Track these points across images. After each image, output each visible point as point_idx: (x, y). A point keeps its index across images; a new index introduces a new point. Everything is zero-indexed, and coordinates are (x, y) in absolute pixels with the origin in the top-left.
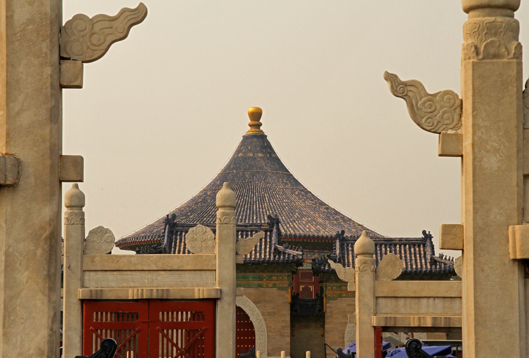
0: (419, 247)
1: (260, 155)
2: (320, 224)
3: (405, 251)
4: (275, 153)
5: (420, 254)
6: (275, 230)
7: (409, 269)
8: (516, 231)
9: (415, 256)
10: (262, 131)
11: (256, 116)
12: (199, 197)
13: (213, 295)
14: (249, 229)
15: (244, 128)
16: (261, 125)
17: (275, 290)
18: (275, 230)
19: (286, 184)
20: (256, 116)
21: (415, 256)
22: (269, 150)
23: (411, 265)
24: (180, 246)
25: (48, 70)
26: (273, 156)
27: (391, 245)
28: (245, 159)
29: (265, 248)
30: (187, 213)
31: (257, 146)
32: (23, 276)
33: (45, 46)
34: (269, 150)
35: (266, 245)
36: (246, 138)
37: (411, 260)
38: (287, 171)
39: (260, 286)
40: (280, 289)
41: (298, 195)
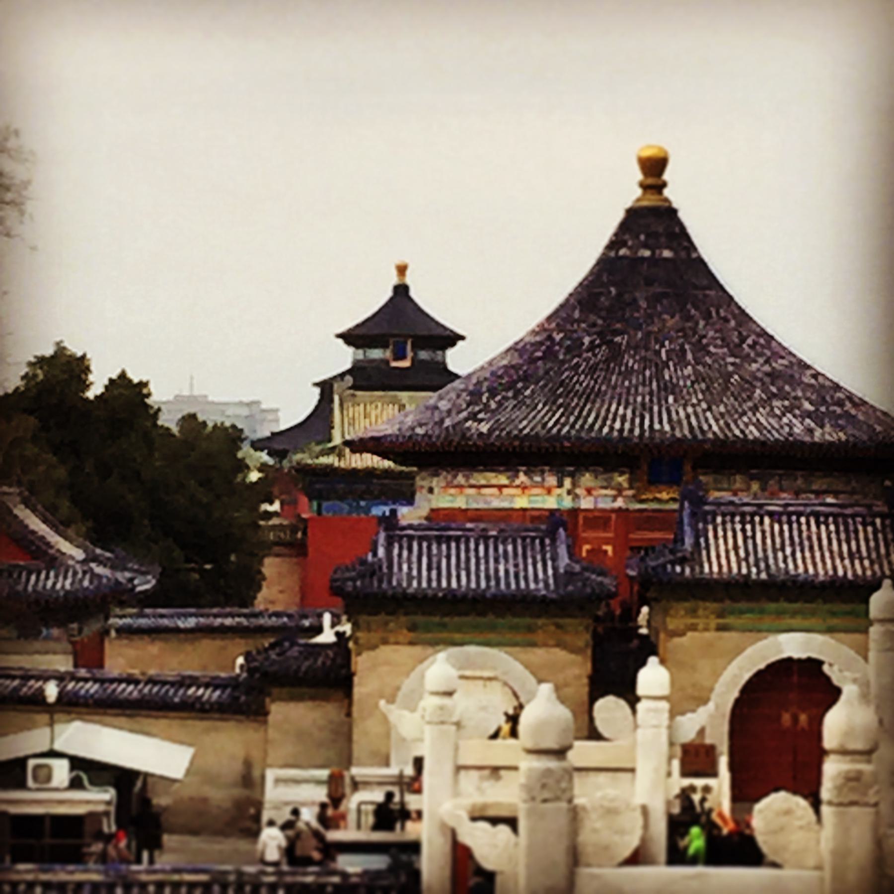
1: (667, 254)
2: (809, 415)
4: (695, 249)
10: (666, 200)
11: (654, 168)
14: (849, 511)
15: (628, 191)
16: (664, 185)
19: (726, 320)
20: (654, 168)
22: (686, 244)
24: (717, 547)
36: (632, 214)
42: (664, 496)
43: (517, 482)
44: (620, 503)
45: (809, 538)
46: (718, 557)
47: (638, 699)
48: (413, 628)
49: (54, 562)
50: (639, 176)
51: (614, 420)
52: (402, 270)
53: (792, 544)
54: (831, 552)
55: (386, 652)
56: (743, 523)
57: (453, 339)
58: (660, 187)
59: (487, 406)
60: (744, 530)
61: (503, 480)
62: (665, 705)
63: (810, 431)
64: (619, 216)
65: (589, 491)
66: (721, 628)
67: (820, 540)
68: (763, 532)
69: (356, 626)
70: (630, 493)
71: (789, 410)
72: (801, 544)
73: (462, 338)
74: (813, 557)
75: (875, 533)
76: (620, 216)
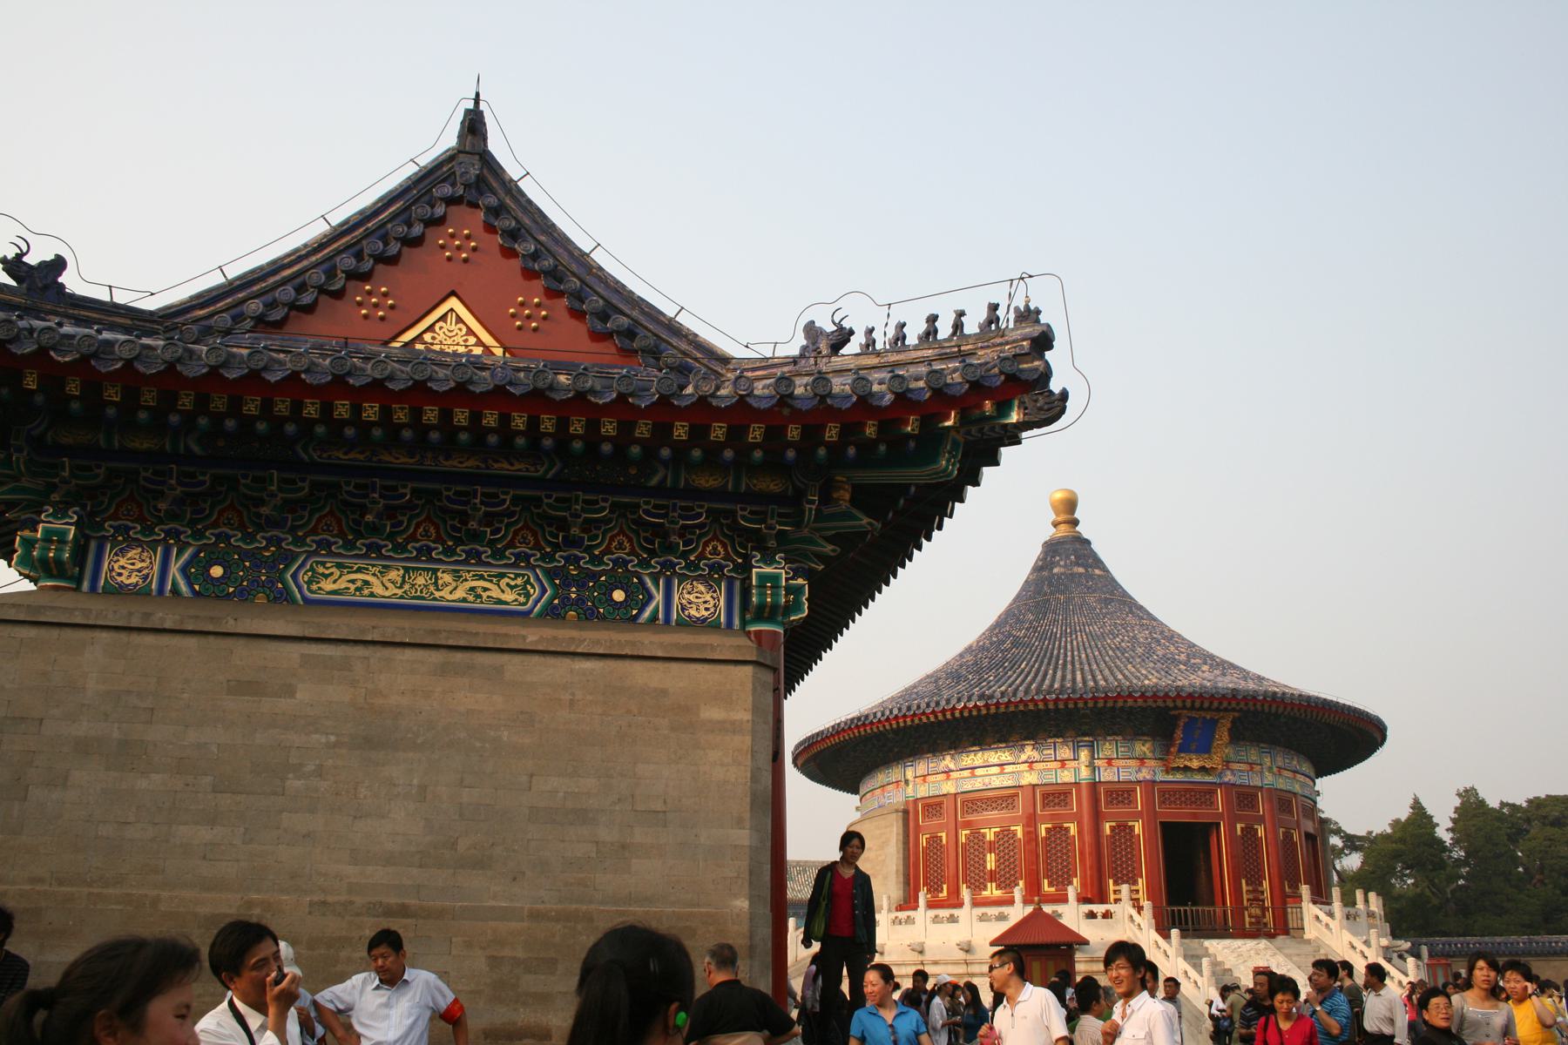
15: (1044, 529)
20: (1070, 505)
36: (1052, 549)
42: (1195, 764)
43: (1024, 757)
44: (1145, 774)
58: (1075, 523)
61: (1005, 756)
65: (1110, 761)
70: (1153, 763)
76: (1037, 551)
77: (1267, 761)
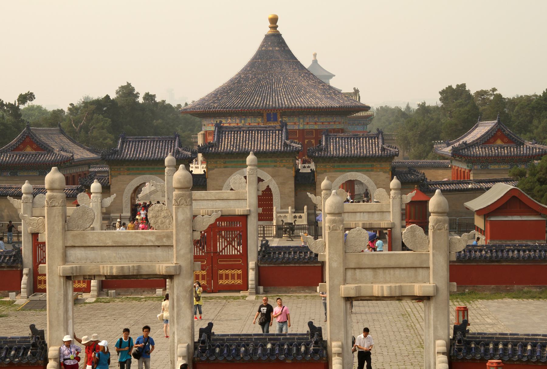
0: (375, 139)
1: (277, 48)
2: (318, 98)
3: (366, 142)
4: (287, 46)
5: (375, 144)
6: (284, 130)
7: (368, 155)
8: (342, 287)
9: (372, 146)
10: (278, 31)
11: (274, 21)
12: (236, 79)
13: (246, 213)
14: (268, 129)
15: (266, 29)
16: (277, 27)
17: (284, 169)
18: (284, 130)
19: (295, 69)
20: (274, 21)
21: (372, 146)
23: (369, 152)
24: (225, 141)
25: (189, 236)
26: (286, 49)
27: (357, 138)
28: (267, 52)
29: (278, 142)
30: (228, 91)
31: (275, 42)
32: (183, 303)
33: (188, 228)
34: (283, 45)
35: (278, 140)
36: (267, 37)
37: (369, 148)
38: (296, 59)
39: (275, 166)
40: (288, 168)
41: (303, 77)
45: (255, 138)
46: (224, 145)
47: (91, 193)
48: (128, 170)
49: (50, 151)
50: (269, 24)
51: (255, 102)
52: (315, 55)
53: (249, 140)
54: (260, 142)
55: (120, 178)
56: (234, 134)
57: (331, 76)
59: (218, 98)
60: (234, 136)
62: (99, 195)
63: (317, 103)
64: (263, 37)
66: (225, 167)
67: (258, 138)
68: (240, 137)
69: (111, 169)
71: (311, 97)
72: (252, 140)
73: (334, 76)
74: (254, 144)
75: (275, 136)
77: (301, 121)
